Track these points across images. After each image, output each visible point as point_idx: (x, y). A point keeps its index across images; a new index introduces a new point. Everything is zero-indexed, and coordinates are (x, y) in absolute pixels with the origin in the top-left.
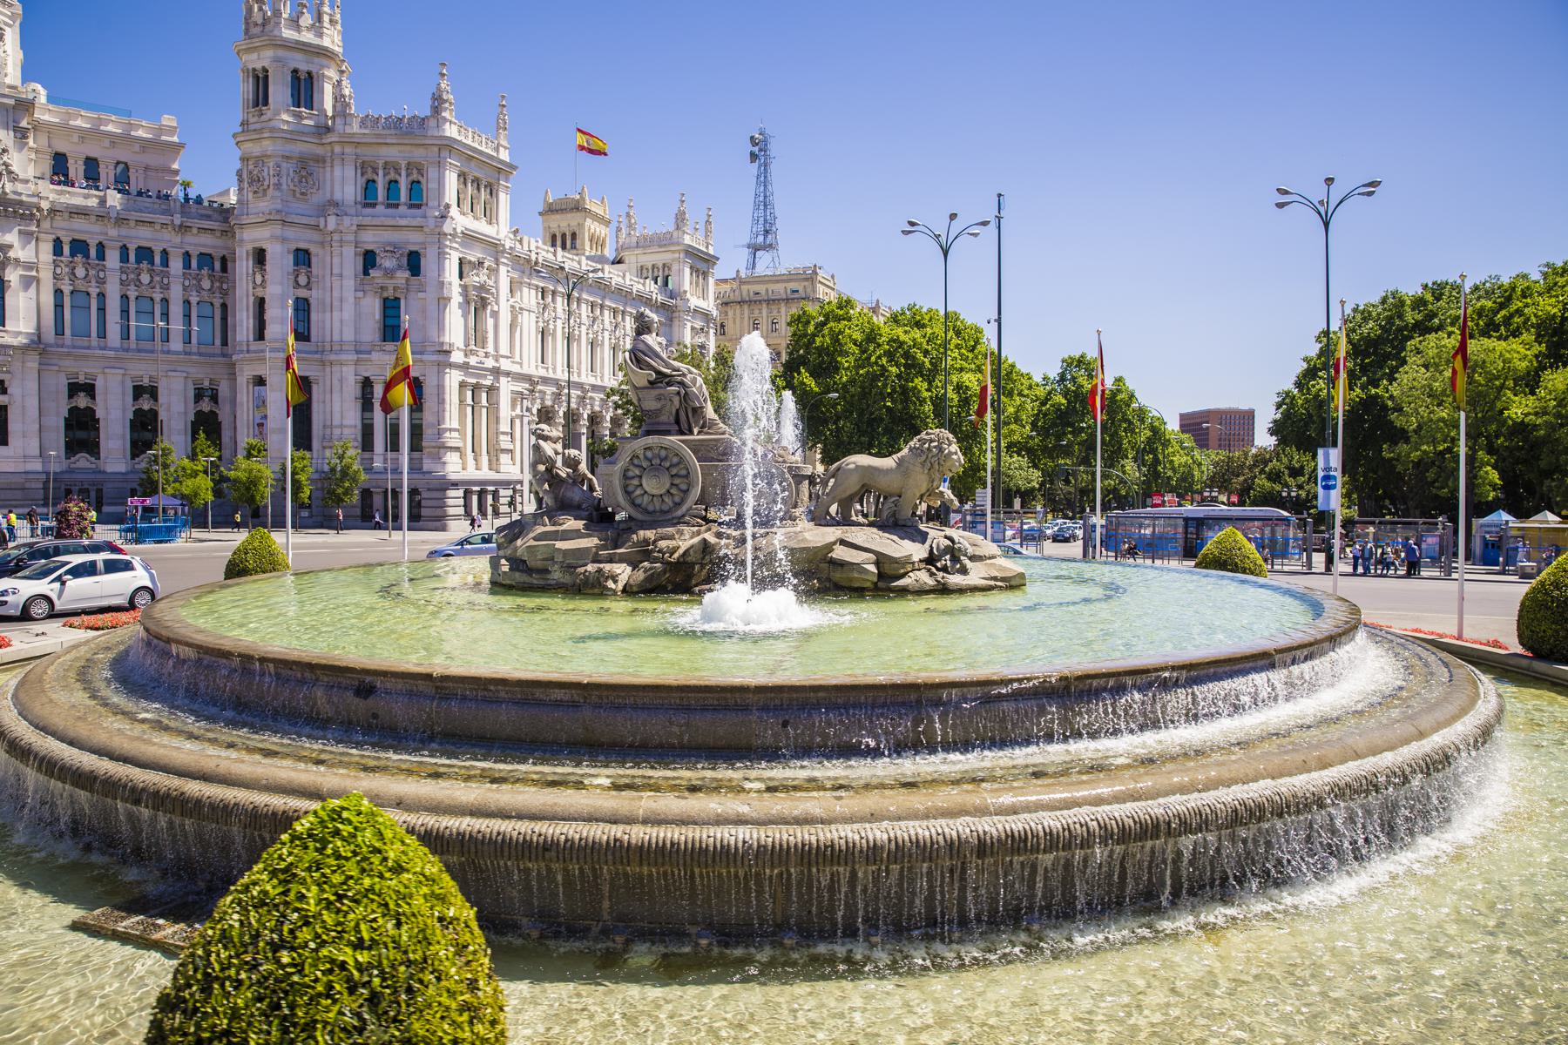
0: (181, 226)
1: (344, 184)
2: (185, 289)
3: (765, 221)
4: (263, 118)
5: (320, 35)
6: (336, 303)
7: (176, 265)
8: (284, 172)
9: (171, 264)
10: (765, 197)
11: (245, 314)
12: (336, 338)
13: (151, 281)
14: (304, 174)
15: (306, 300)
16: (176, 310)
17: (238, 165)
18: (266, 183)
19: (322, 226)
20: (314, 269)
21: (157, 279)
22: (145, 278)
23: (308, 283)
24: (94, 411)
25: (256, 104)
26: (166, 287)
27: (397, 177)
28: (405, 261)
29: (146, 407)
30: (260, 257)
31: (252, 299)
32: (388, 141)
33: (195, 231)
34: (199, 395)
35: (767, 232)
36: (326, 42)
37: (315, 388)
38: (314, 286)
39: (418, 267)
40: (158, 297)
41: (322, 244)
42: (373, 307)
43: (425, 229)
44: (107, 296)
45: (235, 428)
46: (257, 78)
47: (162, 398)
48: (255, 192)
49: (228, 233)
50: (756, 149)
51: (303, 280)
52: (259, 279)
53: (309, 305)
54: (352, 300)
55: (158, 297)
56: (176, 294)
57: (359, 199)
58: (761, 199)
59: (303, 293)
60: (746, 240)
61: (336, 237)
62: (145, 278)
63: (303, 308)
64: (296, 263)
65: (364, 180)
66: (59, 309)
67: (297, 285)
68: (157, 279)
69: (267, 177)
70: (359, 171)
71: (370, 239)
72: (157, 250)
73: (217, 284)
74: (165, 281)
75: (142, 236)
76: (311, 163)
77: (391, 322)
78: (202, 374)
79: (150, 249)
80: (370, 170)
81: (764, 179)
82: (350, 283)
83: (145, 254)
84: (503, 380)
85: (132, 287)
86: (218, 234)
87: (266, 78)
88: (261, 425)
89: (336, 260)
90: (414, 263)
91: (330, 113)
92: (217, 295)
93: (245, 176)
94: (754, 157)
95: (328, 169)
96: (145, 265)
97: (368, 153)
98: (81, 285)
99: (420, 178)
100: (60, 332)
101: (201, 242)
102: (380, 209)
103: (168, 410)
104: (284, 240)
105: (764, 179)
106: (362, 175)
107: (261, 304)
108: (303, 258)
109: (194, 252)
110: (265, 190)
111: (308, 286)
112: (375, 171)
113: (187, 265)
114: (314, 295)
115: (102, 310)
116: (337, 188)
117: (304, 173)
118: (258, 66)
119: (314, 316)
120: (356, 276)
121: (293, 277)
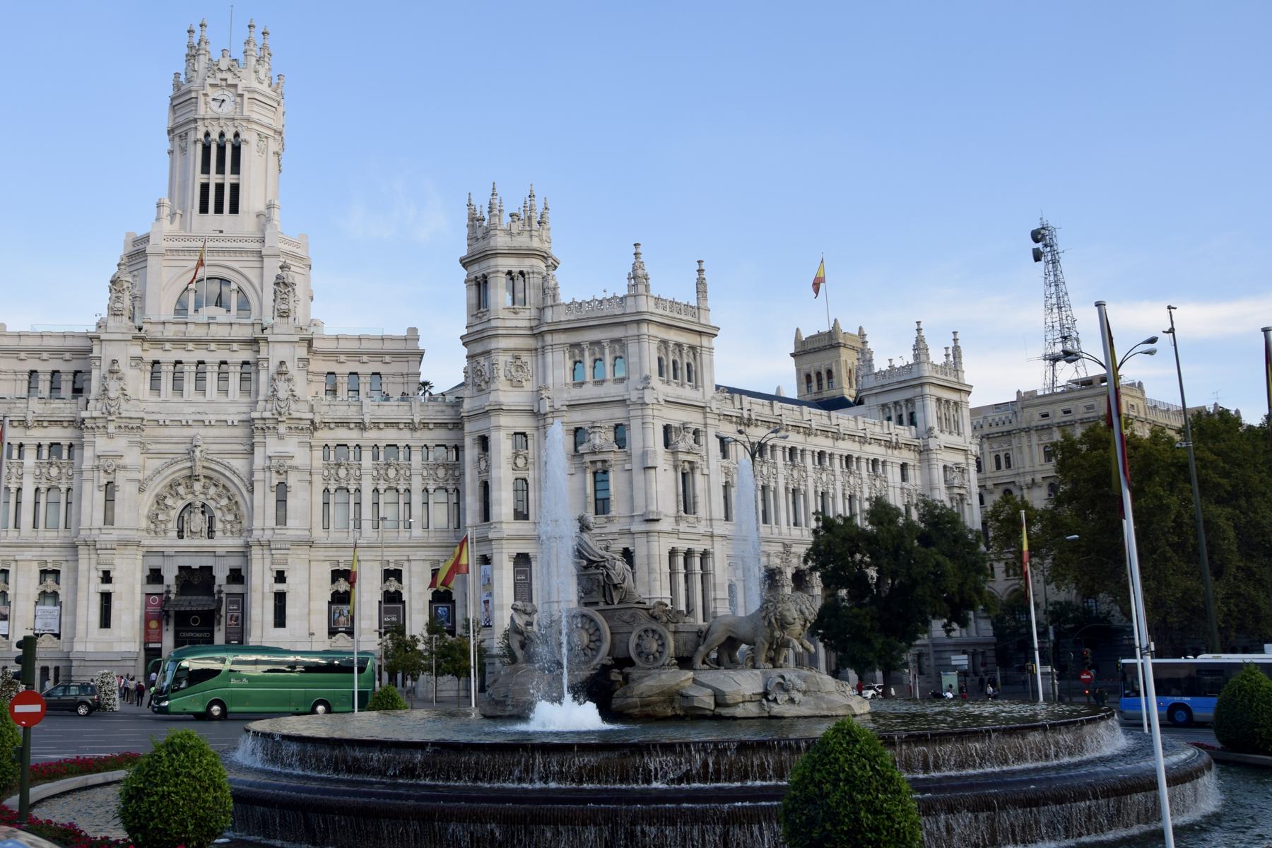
0: (420, 423)
3: (1062, 326)
4: (485, 319)
7: (417, 458)
9: (412, 457)
10: (1058, 298)
14: (519, 363)
15: (525, 480)
16: (417, 498)
17: (465, 363)
19: (535, 411)
22: (392, 473)
27: (602, 357)
28: (611, 436)
29: (392, 589)
30: (484, 442)
31: (478, 483)
32: (591, 323)
33: (431, 426)
35: (1065, 338)
37: (533, 564)
38: (530, 466)
39: (624, 440)
43: (628, 402)
44: (363, 491)
45: (466, 606)
46: (478, 285)
49: (458, 425)
50: (1040, 245)
51: (520, 462)
52: (483, 464)
53: (527, 484)
55: (401, 488)
56: (417, 484)
58: (1054, 301)
59: (521, 474)
60: (1041, 353)
63: (522, 487)
64: (515, 447)
66: (326, 506)
67: (515, 467)
68: (402, 472)
70: (567, 355)
71: (579, 418)
73: (451, 472)
77: (600, 495)
79: (396, 445)
81: (1055, 282)
85: (382, 482)
87: (486, 282)
88: (486, 602)
90: (620, 432)
92: (450, 482)
94: (1037, 256)
95: (540, 357)
100: (326, 526)
103: (410, 591)
105: (1055, 282)
112: (582, 351)
115: (359, 504)
117: (519, 363)
118: (479, 275)
121: (512, 460)
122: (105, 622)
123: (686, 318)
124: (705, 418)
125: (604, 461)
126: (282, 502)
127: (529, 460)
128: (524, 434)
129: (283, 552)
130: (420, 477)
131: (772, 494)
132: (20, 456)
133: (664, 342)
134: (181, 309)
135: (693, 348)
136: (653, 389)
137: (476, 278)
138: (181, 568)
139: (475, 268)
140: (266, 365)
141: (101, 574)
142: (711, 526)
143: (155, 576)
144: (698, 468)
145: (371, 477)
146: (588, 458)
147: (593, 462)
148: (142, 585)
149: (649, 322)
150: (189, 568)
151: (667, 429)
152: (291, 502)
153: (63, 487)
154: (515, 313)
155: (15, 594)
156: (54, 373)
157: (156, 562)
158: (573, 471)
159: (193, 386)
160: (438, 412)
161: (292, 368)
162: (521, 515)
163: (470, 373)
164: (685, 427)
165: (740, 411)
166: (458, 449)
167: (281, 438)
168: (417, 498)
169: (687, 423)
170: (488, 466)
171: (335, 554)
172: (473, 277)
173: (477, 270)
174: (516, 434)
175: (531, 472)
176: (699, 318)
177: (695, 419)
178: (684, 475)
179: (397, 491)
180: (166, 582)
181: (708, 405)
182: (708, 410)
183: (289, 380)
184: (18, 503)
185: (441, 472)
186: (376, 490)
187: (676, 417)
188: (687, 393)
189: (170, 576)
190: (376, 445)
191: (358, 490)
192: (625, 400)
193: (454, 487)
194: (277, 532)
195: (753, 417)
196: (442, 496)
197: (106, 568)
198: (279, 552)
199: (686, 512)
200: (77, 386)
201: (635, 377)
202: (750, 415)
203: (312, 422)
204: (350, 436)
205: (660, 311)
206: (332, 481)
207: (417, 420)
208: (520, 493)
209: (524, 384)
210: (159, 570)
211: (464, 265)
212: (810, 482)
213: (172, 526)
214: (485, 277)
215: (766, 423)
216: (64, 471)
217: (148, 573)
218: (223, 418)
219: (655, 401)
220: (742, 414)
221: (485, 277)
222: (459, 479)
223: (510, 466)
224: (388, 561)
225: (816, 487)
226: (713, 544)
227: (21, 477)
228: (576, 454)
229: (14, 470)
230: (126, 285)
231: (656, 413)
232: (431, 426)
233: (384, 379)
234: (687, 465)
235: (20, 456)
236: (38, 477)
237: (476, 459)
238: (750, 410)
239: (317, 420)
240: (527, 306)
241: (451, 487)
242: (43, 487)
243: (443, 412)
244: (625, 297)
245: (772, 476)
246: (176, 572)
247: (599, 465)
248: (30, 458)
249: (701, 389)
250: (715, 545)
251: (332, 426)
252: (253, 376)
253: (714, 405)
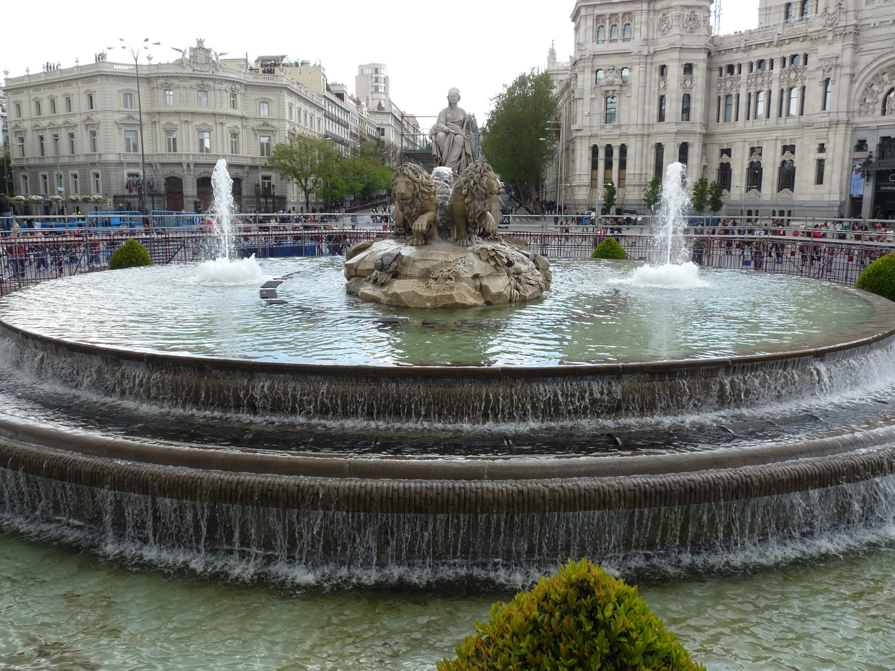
122: (820, 180)
138: (884, 139)
141: (817, 146)
143: (861, 145)
148: (850, 152)
150: (889, 137)
157: (862, 135)
180: (869, 150)
189: (873, 145)
197: (821, 142)
213: (879, 106)
227: (771, 82)
246: (878, 141)
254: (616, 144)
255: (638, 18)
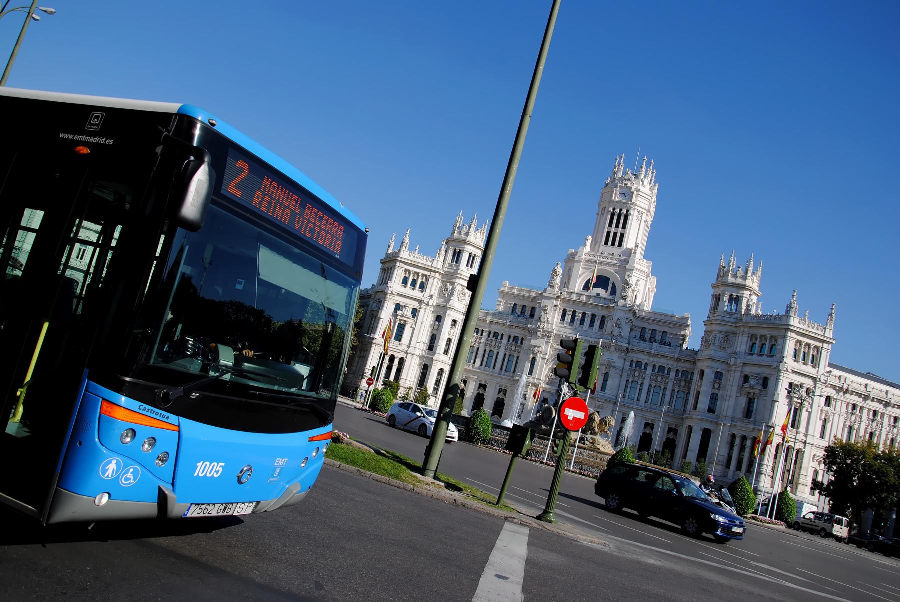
0: (678, 358)
1: (742, 344)
2: (674, 384)
4: (716, 315)
5: (746, 279)
6: (728, 398)
7: (673, 374)
8: (718, 338)
11: (692, 397)
12: (725, 414)
13: (662, 380)
16: (668, 393)
17: (703, 334)
18: (710, 342)
19: (729, 363)
20: (723, 382)
21: (664, 379)
22: (660, 379)
23: (719, 387)
24: (652, 435)
25: (714, 309)
26: (667, 383)
28: (761, 381)
29: (648, 432)
30: (702, 373)
31: (696, 391)
33: (683, 361)
34: (670, 430)
36: (749, 283)
37: (712, 434)
38: (721, 389)
40: (663, 387)
41: (728, 371)
42: (743, 401)
43: (772, 367)
46: (717, 298)
47: (655, 429)
48: (706, 346)
49: (695, 363)
51: (717, 386)
52: (700, 382)
54: (734, 397)
56: (670, 386)
57: (747, 352)
59: (716, 391)
61: (734, 368)
62: (660, 379)
63: (714, 398)
65: (751, 343)
67: (714, 387)
68: (664, 379)
69: (711, 340)
70: (749, 339)
71: (748, 370)
72: (667, 367)
73: (688, 384)
74: (667, 381)
75: (662, 362)
76: (731, 335)
78: (673, 422)
79: (664, 366)
80: (754, 338)
82: (735, 389)
83: (662, 368)
84: (808, 447)
86: (692, 363)
87: (720, 298)
89: (732, 378)
90: (765, 382)
91: (743, 313)
92: (687, 389)
93: (704, 339)
95: (737, 338)
96: (661, 373)
97: (754, 331)
98: (636, 379)
99: (776, 343)
101: (683, 366)
102: (755, 356)
104: (711, 367)
106: (751, 341)
107: (698, 394)
108: (719, 375)
109: (681, 369)
110: (709, 345)
111: (719, 389)
113: (677, 375)
114: (720, 393)
115: (641, 389)
116: (739, 346)
118: (718, 294)
119: (719, 402)
120: (738, 386)
121: (712, 384)
123: (817, 332)
124: (815, 384)
125: (754, 393)
126: (605, 380)
127: (721, 386)
128: (722, 373)
129: (601, 403)
130: (673, 383)
131: (855, 431)
132: (482, 335)
133: (800, 342)
134: (587, 287)
135: (817, 347)
136: (786, 363)
137: (716, 295)
139: (717, 290)
140: (612, 319)
142: (806, 437)
144: (805, 407)
145: (649, 378)
146: (748, 390)
147: (749, 393)
149: (792, 331)
151: (791, 384)
152: (609, 382)
153: (516, 355)
154: (730, 315)
155: (487, 396)
156: (524, 306)
158: (739, 395)
159: (579, 322)
160: (688, 355)
161: (623, 323)
162: (711, 410)
163: (704, 339)
164: (802, 386)
165: (843, 384)
166: (693, 373)
167: (611, 352)
168: (668, 393)
169: (803, 384)
170: (701, 384)
171: (626, 410)
172: (715, 294)
173: (718, 291)
174: (717, 371)
175: (721, 391)
176: (824, 334)
177: (809, 383)
178: (796, 410)
179: (661, 387)
181: (819, 377)
182: (818, 379)
183: (620, 327)
184: (497, 358)
185: (683, 383)
186: (650, 385)
187: (798, 379)
188: (809, 369)
190: (655, 365)
191: (642, 383)
192: (771, 366)
193: (688, 391)
194: (600, 393)
195: (850, 389)
196: (681, 395)
198: (599, 402)
199: (793, 426)
200: (533, 313)
201: (778, 356)
202: (848, 388)
203: (628, 349)
204: (643, 358)
205: (801, 326)
206: (631, 377)
207: (676, 357)
208: (714, 400)
209: (727, 349)
210: (548, 399)
211: (713, 288)
212: (884, 431)
214: (720, 295)
215: (859, 395)
216: (517, 348)
217: (543, 399)
218: (588, 338)
219: (785, 369)
220: (843, 386)
221: (720, 295)
222: (690, 388)
223: (711, 386)
224: (649, 418)
225: (888, 434)
226: (805, 448)
227: (499, 347)
228: (741, 388)
229: (497, 344)
230: (558, 273)
231: (785, 375)
232: (683, 361)
233: (668, 335)
234: (798, 405)
235: (502, 339)
236: (506, 349)
237: (698, 379)
238: (849, 385)
239: (630, 347)
240: (737, 313)
241: (686, 391)
242: (508, 354)
243: (690, 355)
244: (783, 315)
245: (857, 422)
247: (752, 394)
248: (505, 341)
249: (817, 369)
250: (806, 448)
251: (637, 352)
252: (606, 323)
253: (823, 378)
254: (398, 356)
255: (431, 281)
